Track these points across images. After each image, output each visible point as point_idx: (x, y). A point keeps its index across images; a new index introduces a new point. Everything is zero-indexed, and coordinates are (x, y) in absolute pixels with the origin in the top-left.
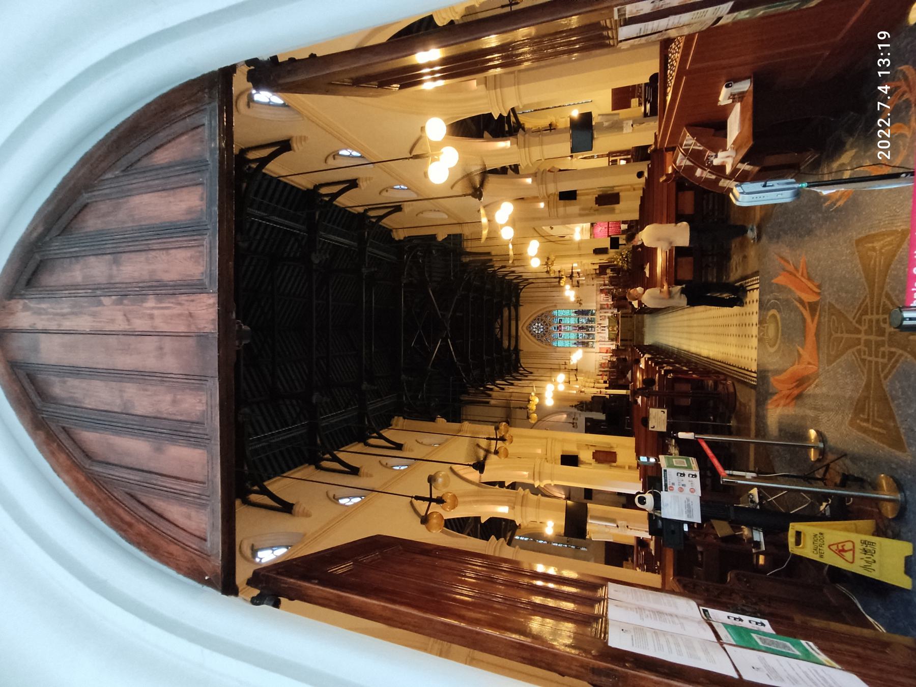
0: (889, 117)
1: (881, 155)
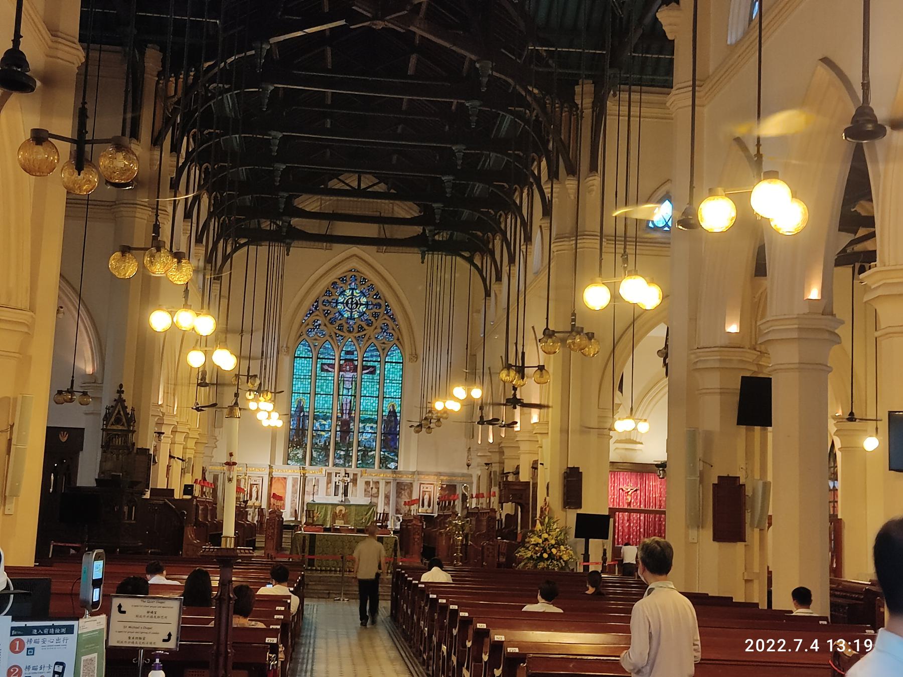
0: (787, 650)
1: (749, 643)
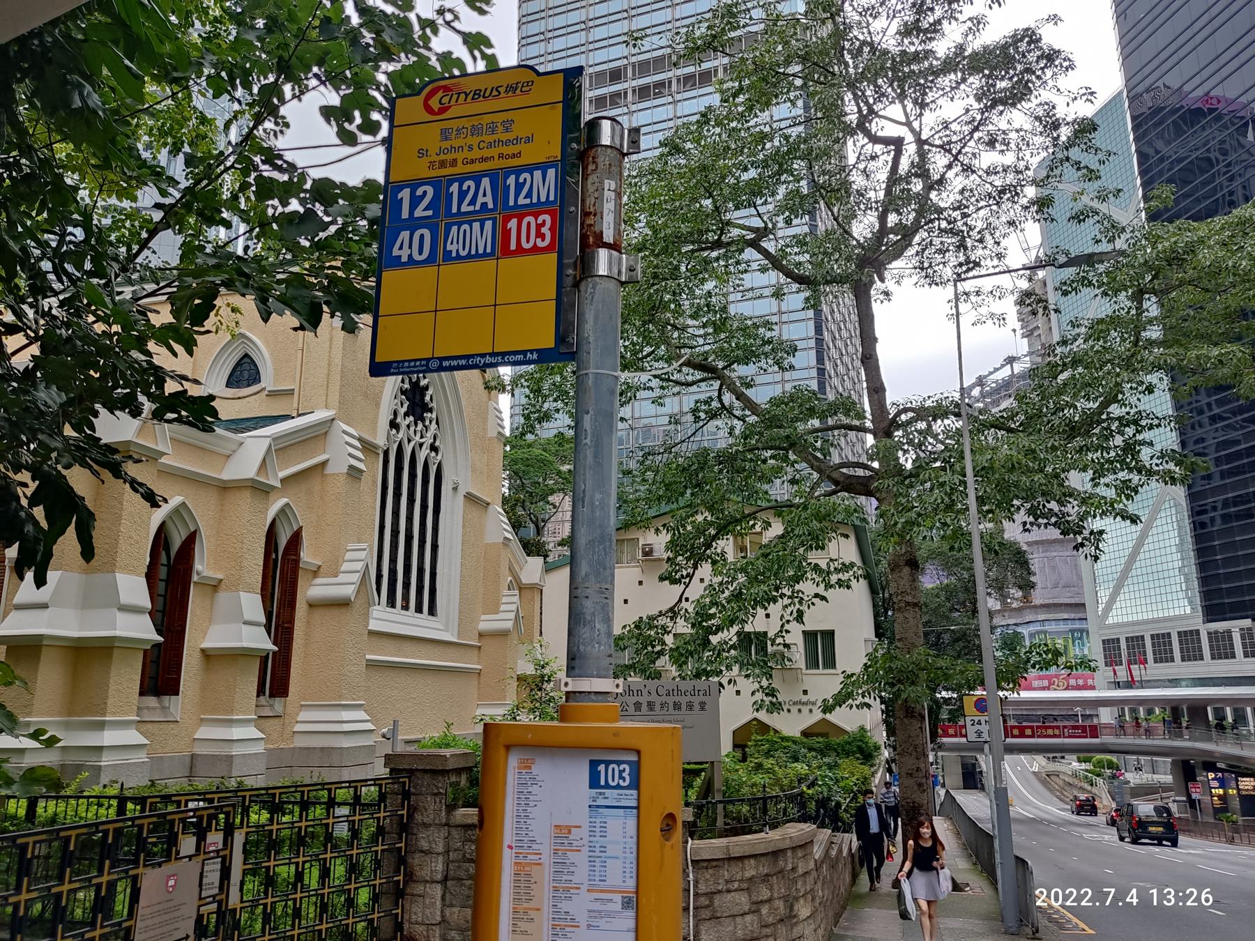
0: (1094, 904)
